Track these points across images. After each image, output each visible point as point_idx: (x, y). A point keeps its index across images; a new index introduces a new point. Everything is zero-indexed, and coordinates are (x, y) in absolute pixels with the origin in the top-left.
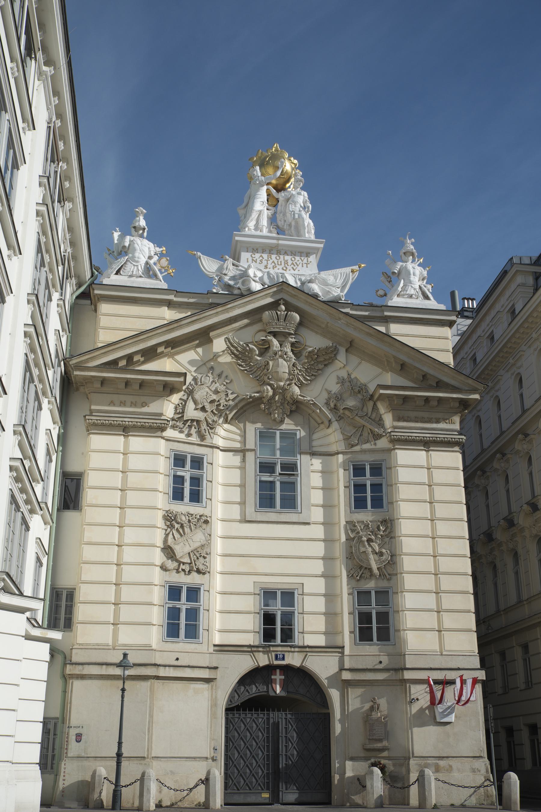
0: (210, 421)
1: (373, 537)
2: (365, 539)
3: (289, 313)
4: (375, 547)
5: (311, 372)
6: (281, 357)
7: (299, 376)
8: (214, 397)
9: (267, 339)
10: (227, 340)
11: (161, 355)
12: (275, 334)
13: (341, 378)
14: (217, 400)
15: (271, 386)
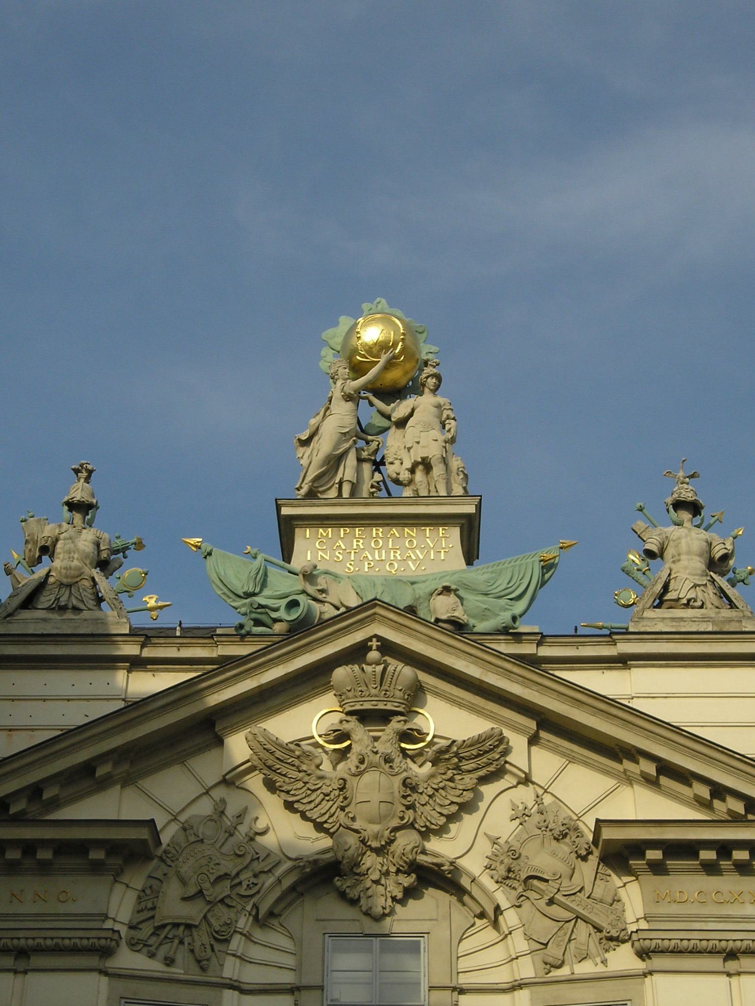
0: (216, 924)
5: (449, 797)
9: (344, 729)
11: (103, 784)
14: (234, 873)
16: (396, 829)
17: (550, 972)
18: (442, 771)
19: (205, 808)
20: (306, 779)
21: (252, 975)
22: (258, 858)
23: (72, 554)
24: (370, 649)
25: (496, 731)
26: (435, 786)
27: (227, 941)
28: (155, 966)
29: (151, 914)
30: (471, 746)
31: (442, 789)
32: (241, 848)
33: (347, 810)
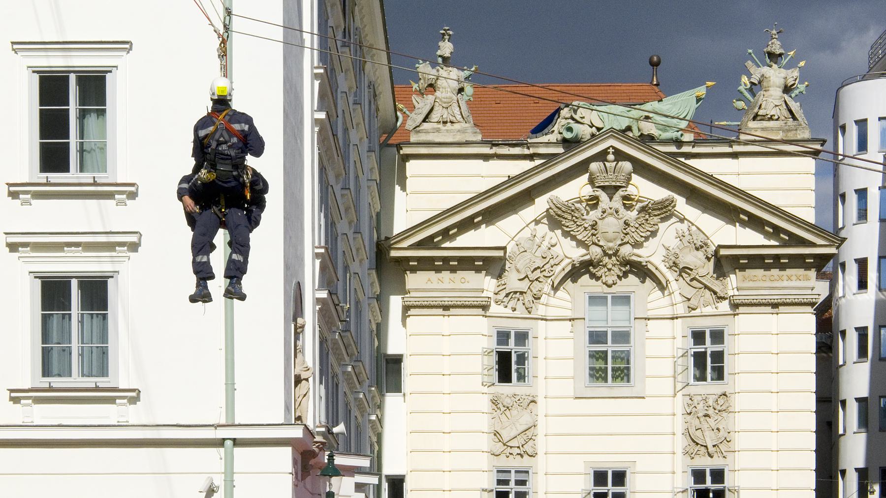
1: (711, 412)
2: (700, 415)
3: (620, 163)
4: (711, 422)
6: (612, 214)
7: (633, 234)
8: (539, 263)
10: (550, 201)
11: (477, 226)
12: (603, 188)
13: (681, 232)
15: (601, 246)
16: (620, 245)
17: (691, 311)
18: (643, 216)
19: (527, 233)
20: (576, 220)
21: (552, 313)
22: (553, 258)
23: (447, 89)
24: (609, 153)
25: (671, 197)
26: (640, 223)
27: (539, 298)
28: (508, 312)
29: (504, 287)
30: (658, 203)
31: (643, 224)
32: (545, 254)
33: (597, 236)
